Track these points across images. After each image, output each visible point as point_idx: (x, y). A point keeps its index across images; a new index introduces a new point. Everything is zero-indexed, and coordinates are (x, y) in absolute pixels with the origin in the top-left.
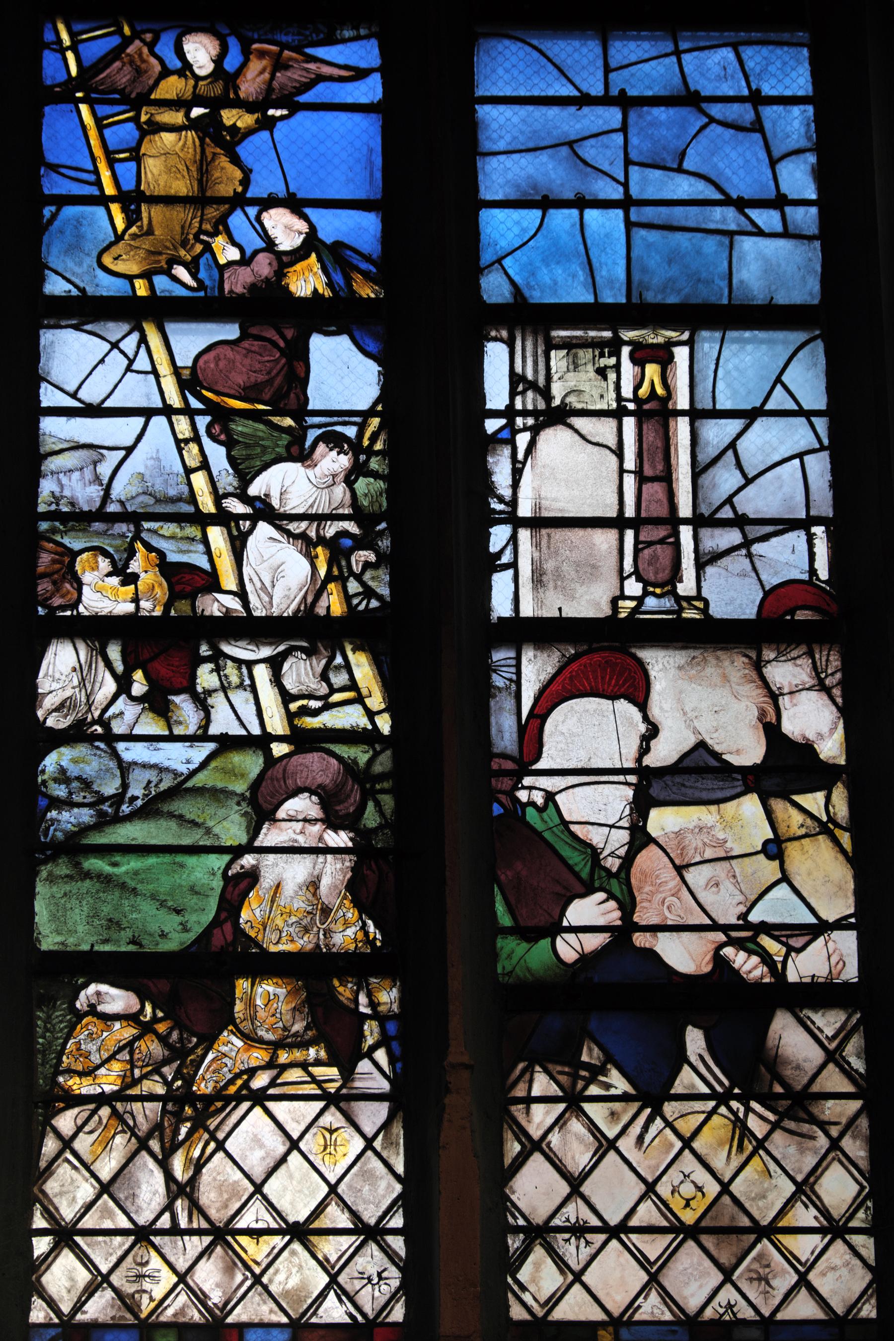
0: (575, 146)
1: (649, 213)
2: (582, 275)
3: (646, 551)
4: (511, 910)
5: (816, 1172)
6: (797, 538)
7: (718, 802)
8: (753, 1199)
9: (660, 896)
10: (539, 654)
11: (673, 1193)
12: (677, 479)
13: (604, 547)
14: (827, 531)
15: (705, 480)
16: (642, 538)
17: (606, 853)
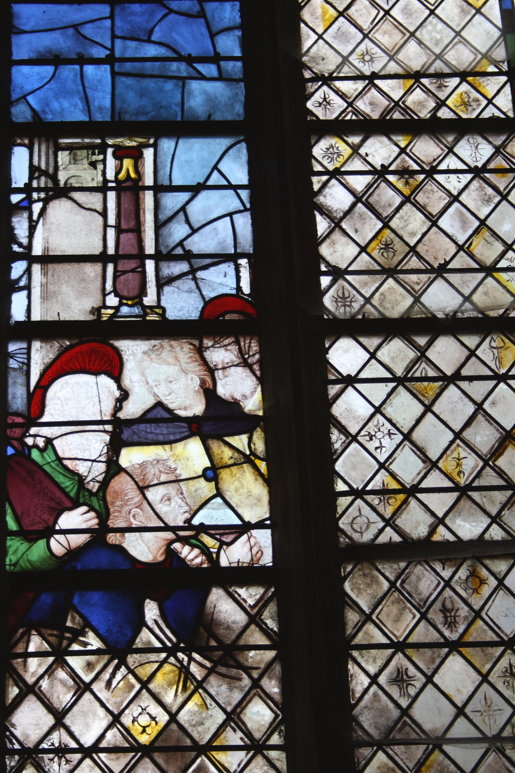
0: (79, 28)
1: (128, 66)
2: (80, 105)
3: (122, 277)
4: (17, 519)
5: (242, 704)
6: (229, 268)
7: (170, 442)
8: (194, 726)
9: (127, 508)
10: (44, 345)
11: (133, 721)
12: (144, 231)
13: (93, 274)
14: (249, 262)
15: (164, 231)
16: (119, 269)
17: (89, 479)
